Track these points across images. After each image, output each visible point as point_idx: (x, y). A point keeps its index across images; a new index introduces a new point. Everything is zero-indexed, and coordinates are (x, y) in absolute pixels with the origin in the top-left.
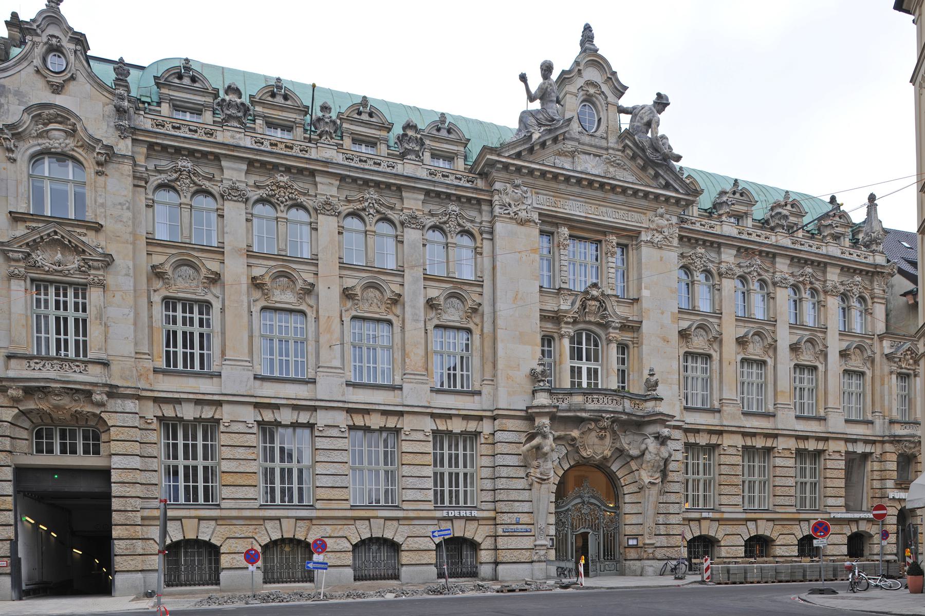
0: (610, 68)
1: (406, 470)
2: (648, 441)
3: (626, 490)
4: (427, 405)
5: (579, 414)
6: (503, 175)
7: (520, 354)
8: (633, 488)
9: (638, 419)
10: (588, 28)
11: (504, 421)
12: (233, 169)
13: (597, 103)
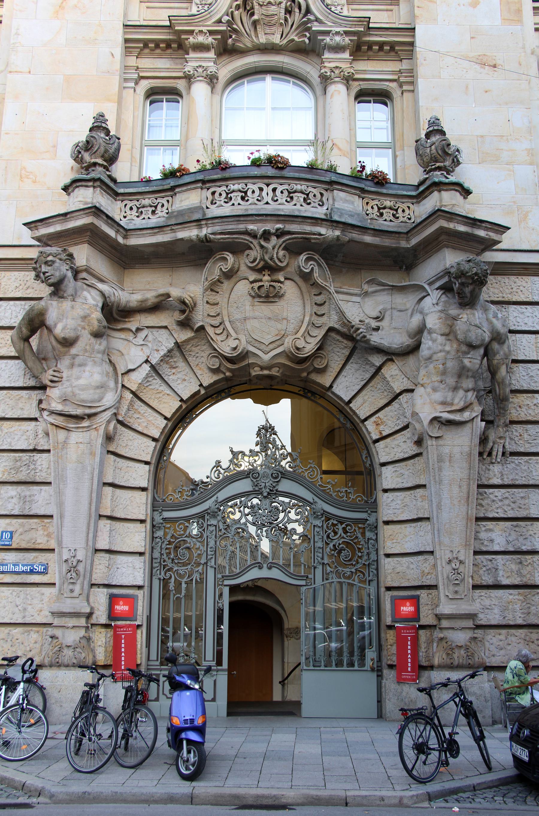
2: (428, 302)
3: (383, 452)
5: (182, 234)
8: (402, 446)
9: (387, 242)
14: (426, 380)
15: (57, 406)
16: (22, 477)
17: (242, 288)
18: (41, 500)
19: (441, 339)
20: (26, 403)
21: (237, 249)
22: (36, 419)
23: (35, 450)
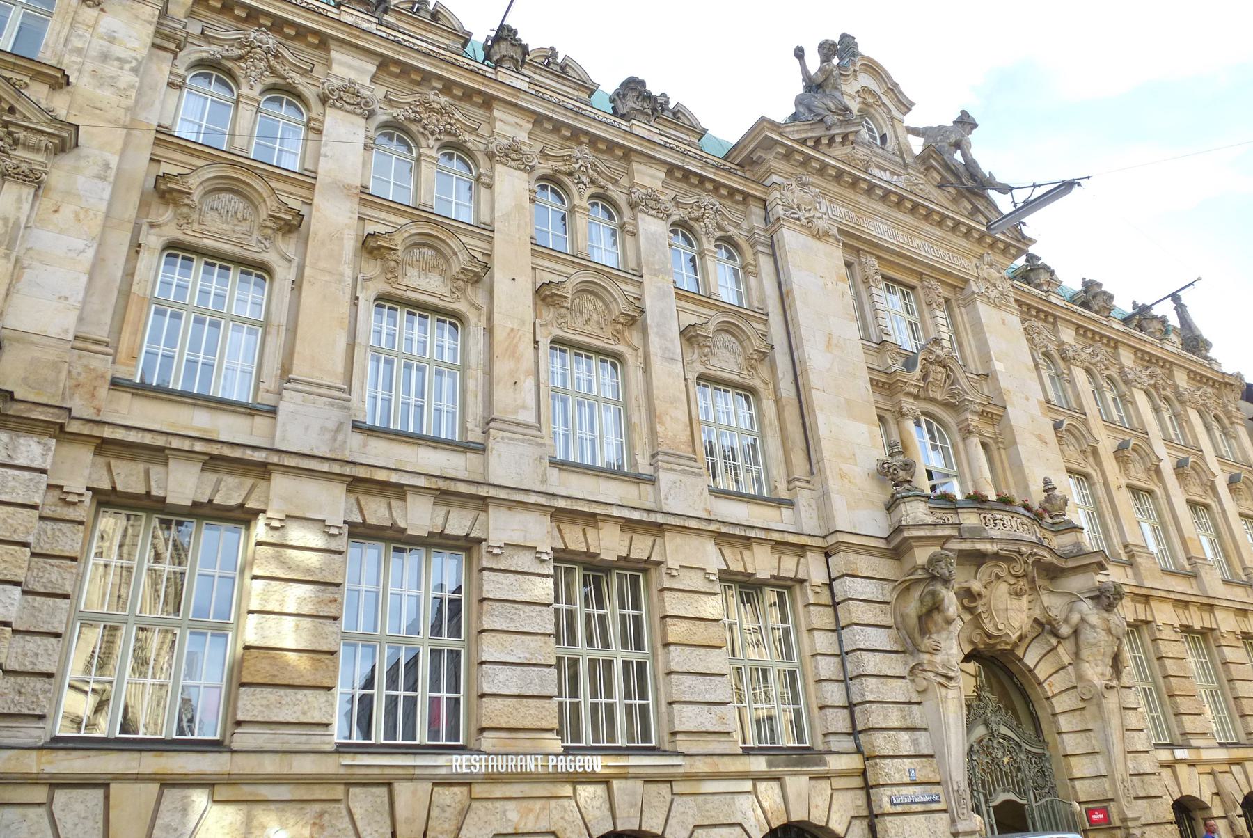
0: (889, 77)
1: (678, 659)
4: (705, 516)
7: (851, 439)
11: (852, 557)
14: (1091, 659)
16: (908, 724)
17: (1003, 588)
19: (1103, 633)
20: (896, 665)
21: (1008, 559)
22: (903, 678)
23: (910, 703)
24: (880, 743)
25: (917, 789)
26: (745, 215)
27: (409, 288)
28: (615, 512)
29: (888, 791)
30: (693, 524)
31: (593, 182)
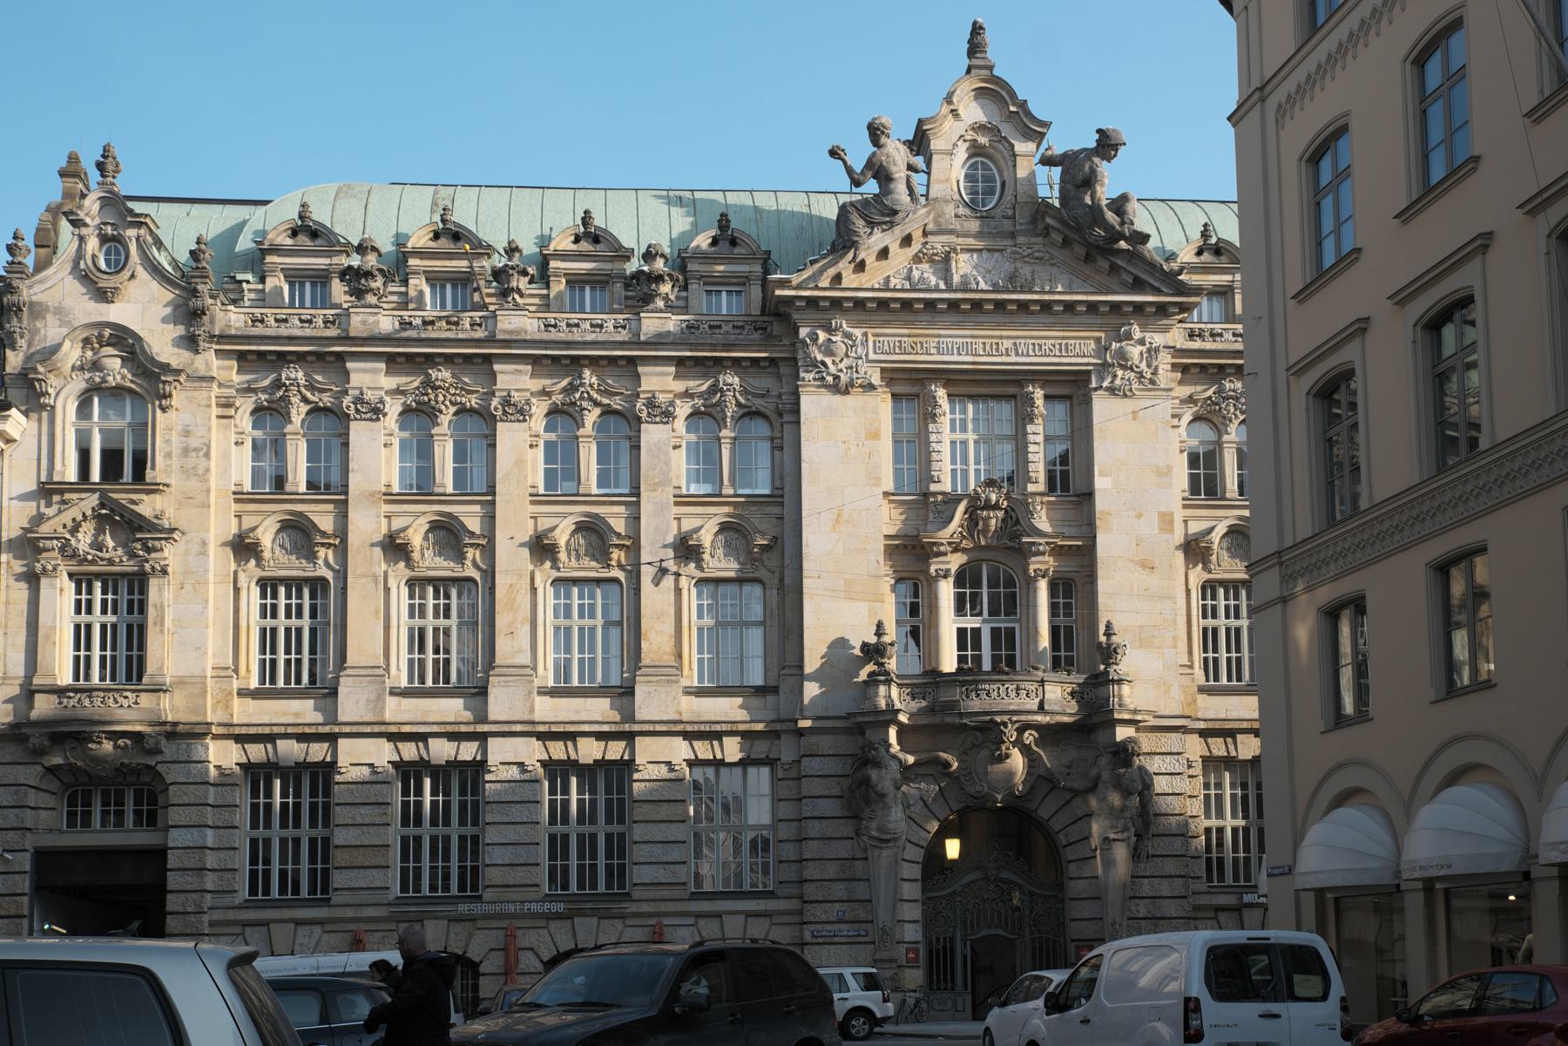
0: (1013, 94)
2: (1103, 761)
6: (811, 314)
10: (977, 29)
12: (365, 371)
13: (998, 156)
15: (874, 833)
18: (861, 890)
20: (846, 829)
24: (811, 891)
25: (844, 926)
26: (779, 377)
27: (429, 569)
28: (586, 728)
29: (812, 927)
30: (658, 728)
31: (597, 404)
